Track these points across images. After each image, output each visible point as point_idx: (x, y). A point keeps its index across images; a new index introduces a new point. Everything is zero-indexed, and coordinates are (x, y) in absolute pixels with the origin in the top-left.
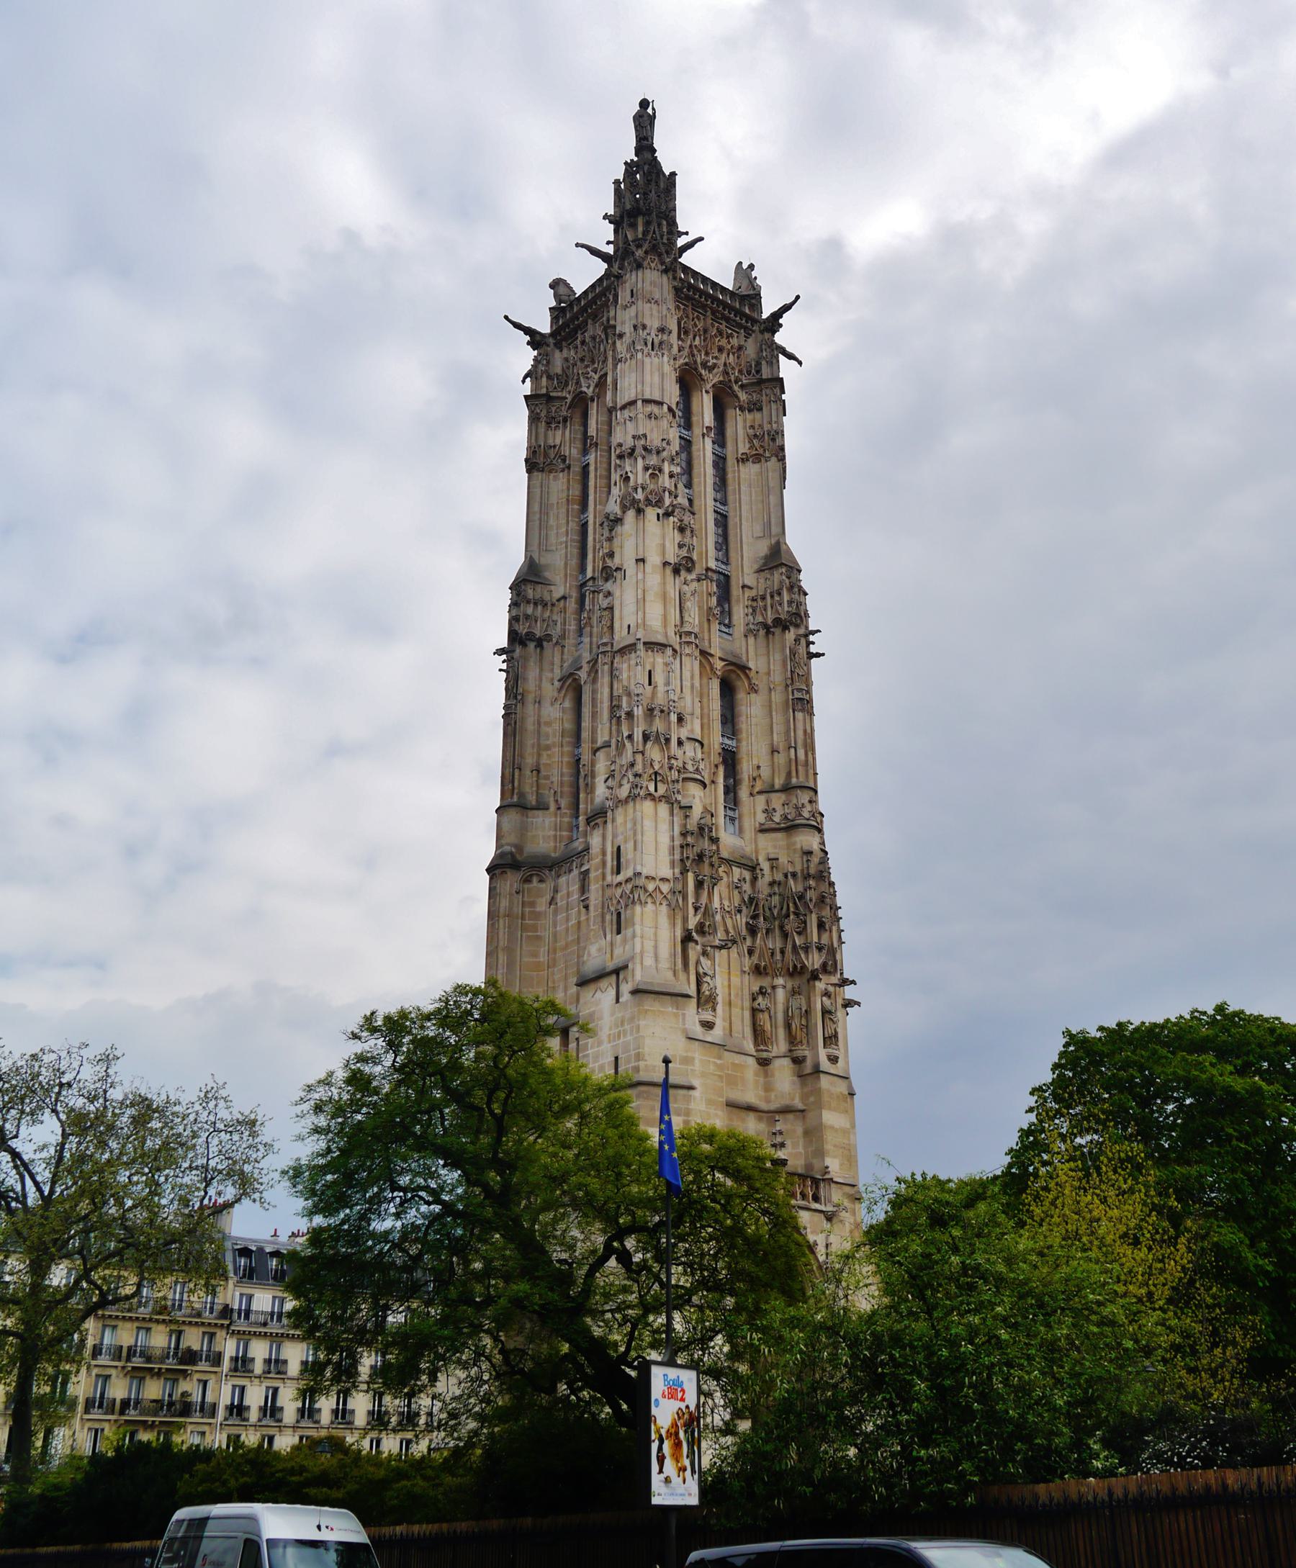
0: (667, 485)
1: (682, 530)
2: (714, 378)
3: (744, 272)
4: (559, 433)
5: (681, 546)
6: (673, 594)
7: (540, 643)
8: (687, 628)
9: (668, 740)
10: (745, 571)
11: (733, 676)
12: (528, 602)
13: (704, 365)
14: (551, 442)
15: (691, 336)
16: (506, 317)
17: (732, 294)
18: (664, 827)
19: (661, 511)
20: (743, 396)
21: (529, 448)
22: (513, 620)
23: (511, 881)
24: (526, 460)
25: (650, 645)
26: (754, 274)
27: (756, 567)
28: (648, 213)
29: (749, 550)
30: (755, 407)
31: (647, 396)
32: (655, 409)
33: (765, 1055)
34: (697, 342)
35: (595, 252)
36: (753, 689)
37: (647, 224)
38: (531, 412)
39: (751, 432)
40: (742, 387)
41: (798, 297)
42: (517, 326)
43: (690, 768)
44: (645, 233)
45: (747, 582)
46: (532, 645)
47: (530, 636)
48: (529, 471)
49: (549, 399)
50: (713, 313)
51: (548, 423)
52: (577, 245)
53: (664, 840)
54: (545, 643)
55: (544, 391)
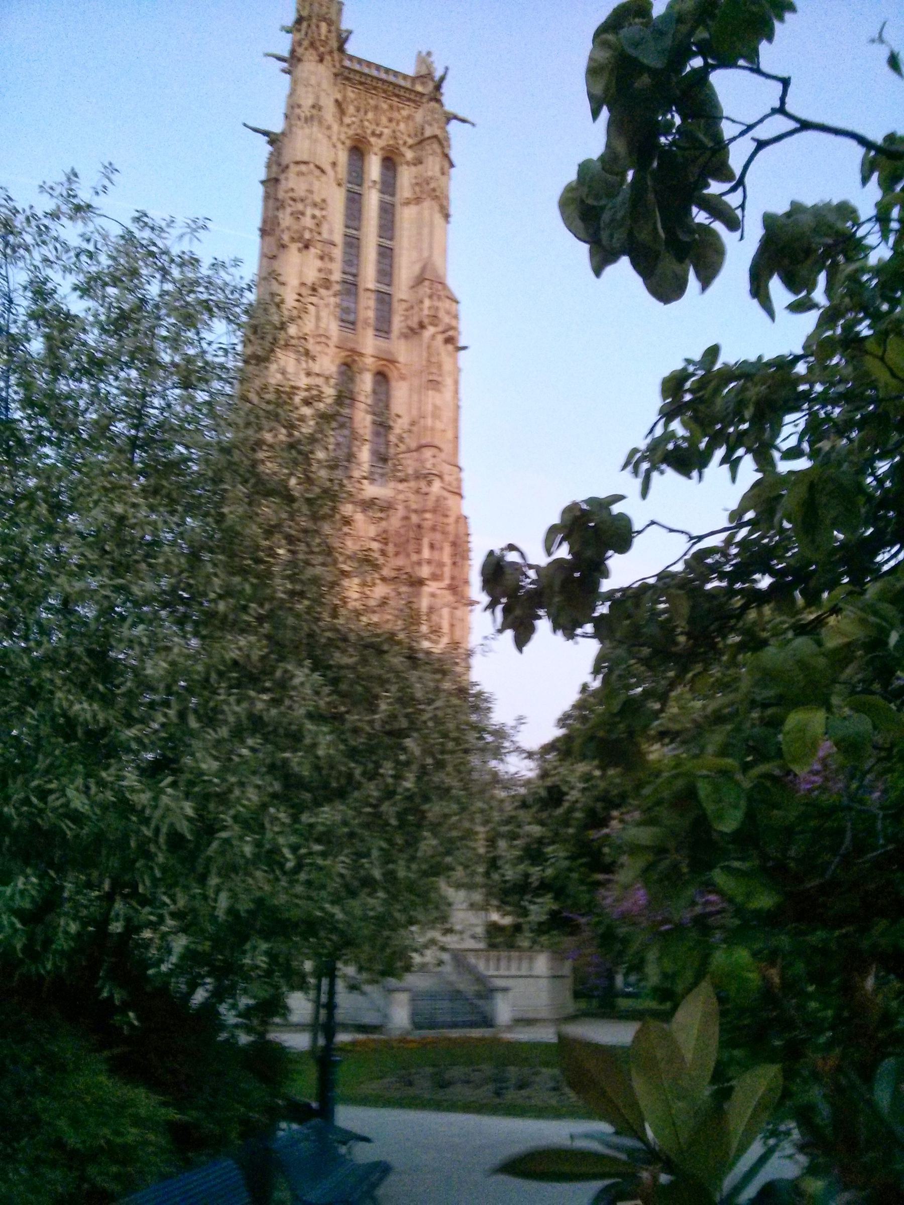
1: (322, 258)
3: (424, 59)
10: (402, 289)
11: (385, 369)
13: (373, 134)
15: (362, 112)
16: (245, 125)
17: (405, 77)
19: (300, 245)
20: (409, 155)
26: (431, 59)
27: (411, 284)
28: (310, 18)
29: (406, 269)
30: (418, 162)
31: (298, 159)
32: (303, 168)
34: (370, 115)
35: (280, 59)
36: (403, 378)
37: (309, 26)
39: (414, 181)
40: (410, 147)
41: (447, 69)
42: (256, 130)
44: (306, 34)
45: (404, 297)
50: (385, 92)
52: (267, 55)
55: (273, 176)
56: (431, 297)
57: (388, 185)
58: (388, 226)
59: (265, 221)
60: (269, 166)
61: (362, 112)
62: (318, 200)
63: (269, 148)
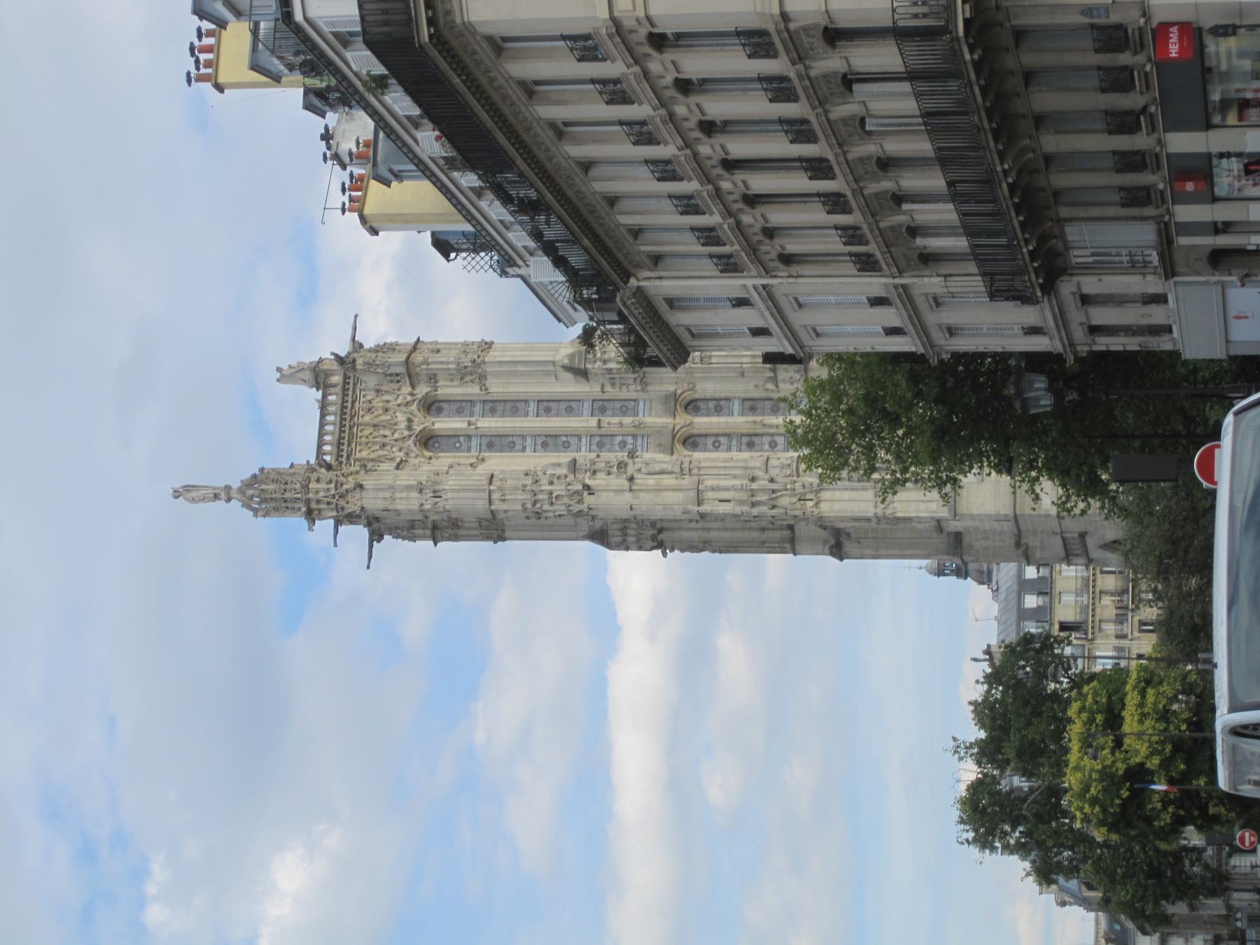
5: (609, 473)
6: (651, 481)
7: (660, 531)
8: (677, 469)
9: (774, 491)
11: (684, 403)
22: (640, 548)
23: (848, 547)
24: (495, 542)
26: (285, 367)
27: (583, 381)
34: (387, 432)
38: (448, 539)
42: (370, 557)
43: (788, 472)
45: (599, 389)
46: (661, 536)
47: (654, 538)
48: (504, 539)
50: (352, 417)
51: (458, 527)
54: (658, 526)
55: (428, 532)
56: (605, 362)
57: (462, 406)
58: (515, 406)
59: (488, 538)
60: (413, 538)
61: (386, 440)
62: (529, 481)
63: (387, 538)
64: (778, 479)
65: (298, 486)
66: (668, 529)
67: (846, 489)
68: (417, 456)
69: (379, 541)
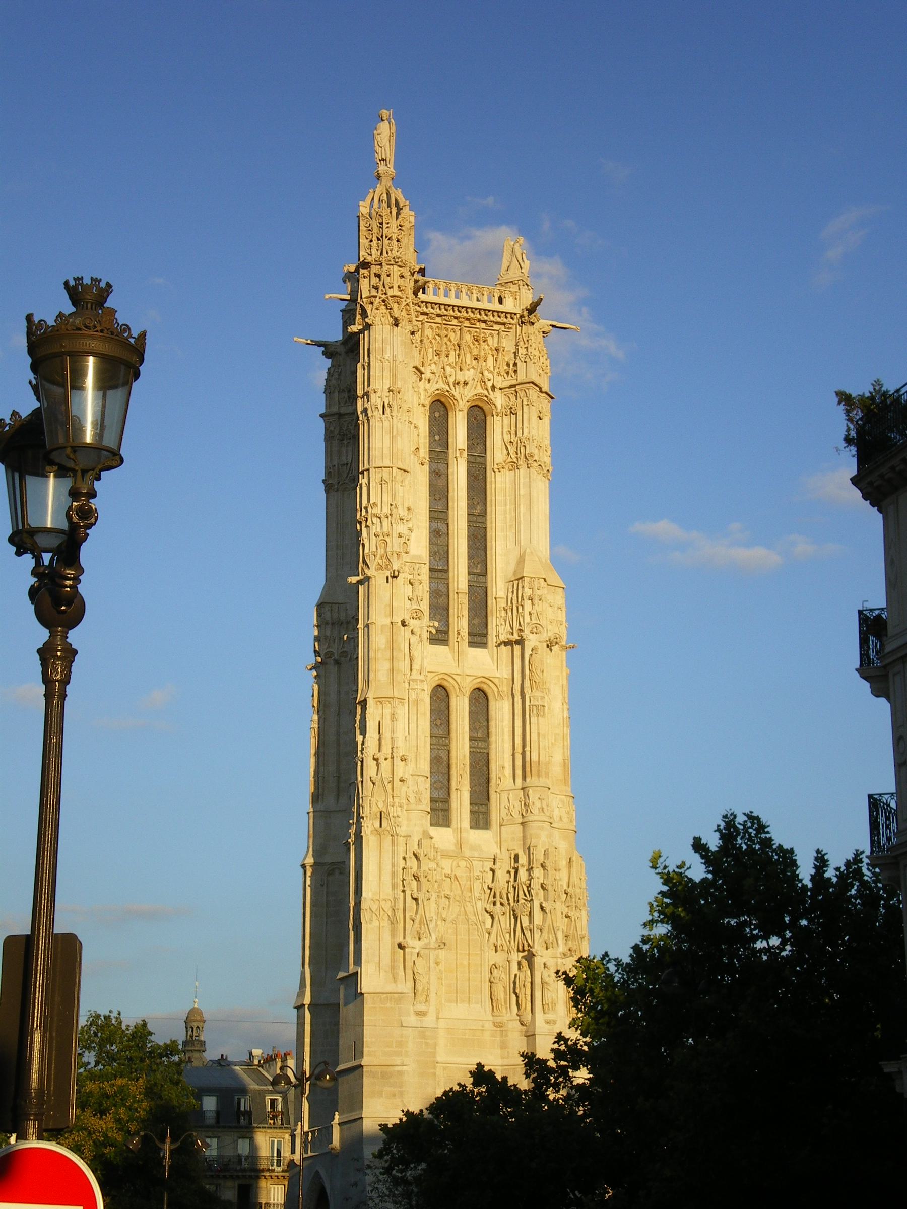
0: (396, 548)
2: (463, 398)
4: (350, 449)
7: (337, 662)
12: (327, 623)
14: (344, 460)
18: (387, 856)
21: (326, 467)
24: (324, 481)
25: (379, 700)
33: (498, 1019)
34: (452, 358)
38: (326, 429)
48: (327, 491)
49: (340, 415)
53: (387, 868)
55: (335, 409)
59: (328, 473)
62: (402, 512)
63: (328, 363)
64: (404, 789)
65: (395, 254)
66: (339, 668)
67: (393, 865)
68: (426, 390)
69: (324, 353)
